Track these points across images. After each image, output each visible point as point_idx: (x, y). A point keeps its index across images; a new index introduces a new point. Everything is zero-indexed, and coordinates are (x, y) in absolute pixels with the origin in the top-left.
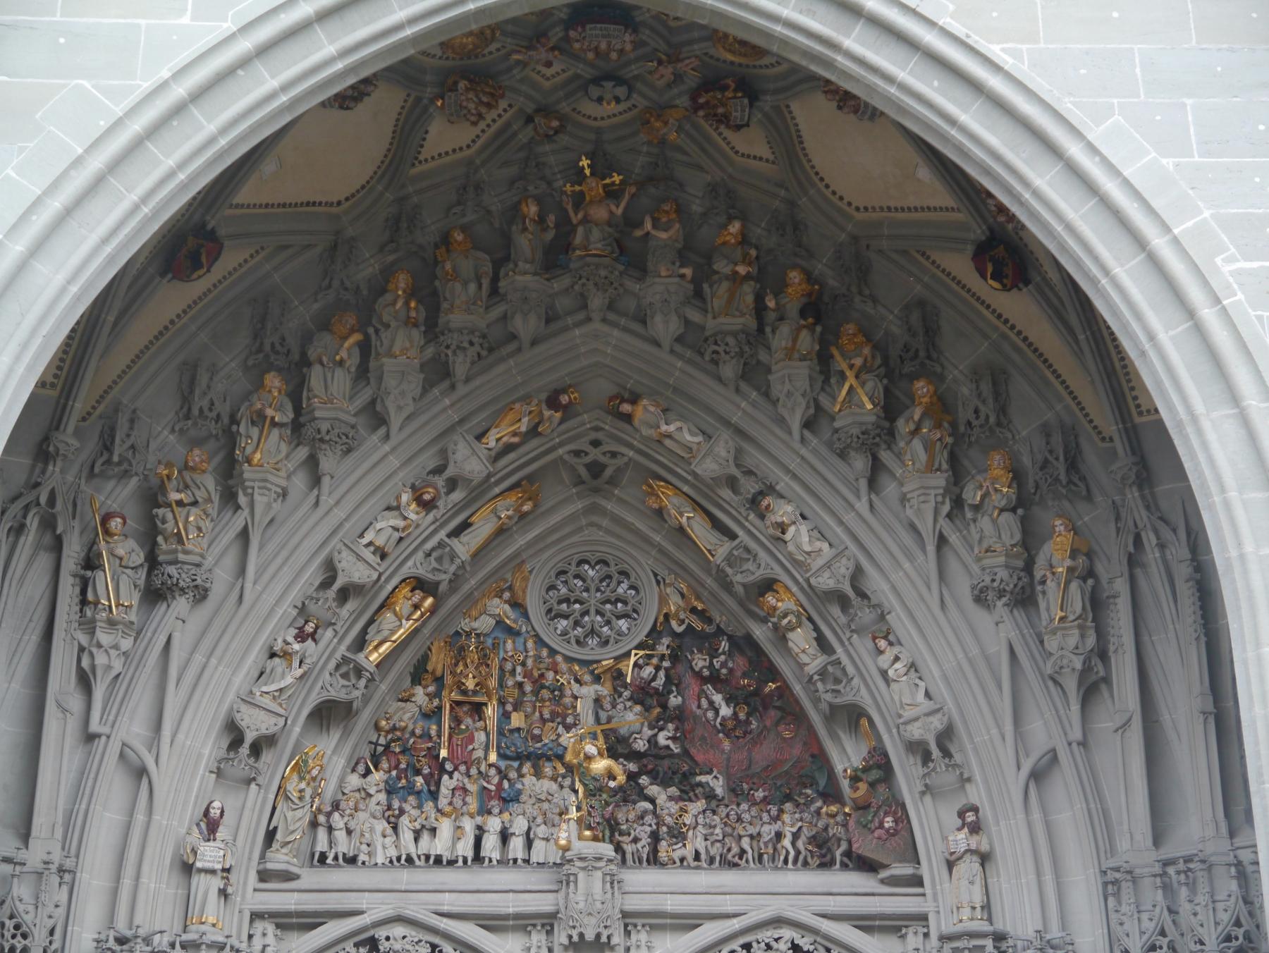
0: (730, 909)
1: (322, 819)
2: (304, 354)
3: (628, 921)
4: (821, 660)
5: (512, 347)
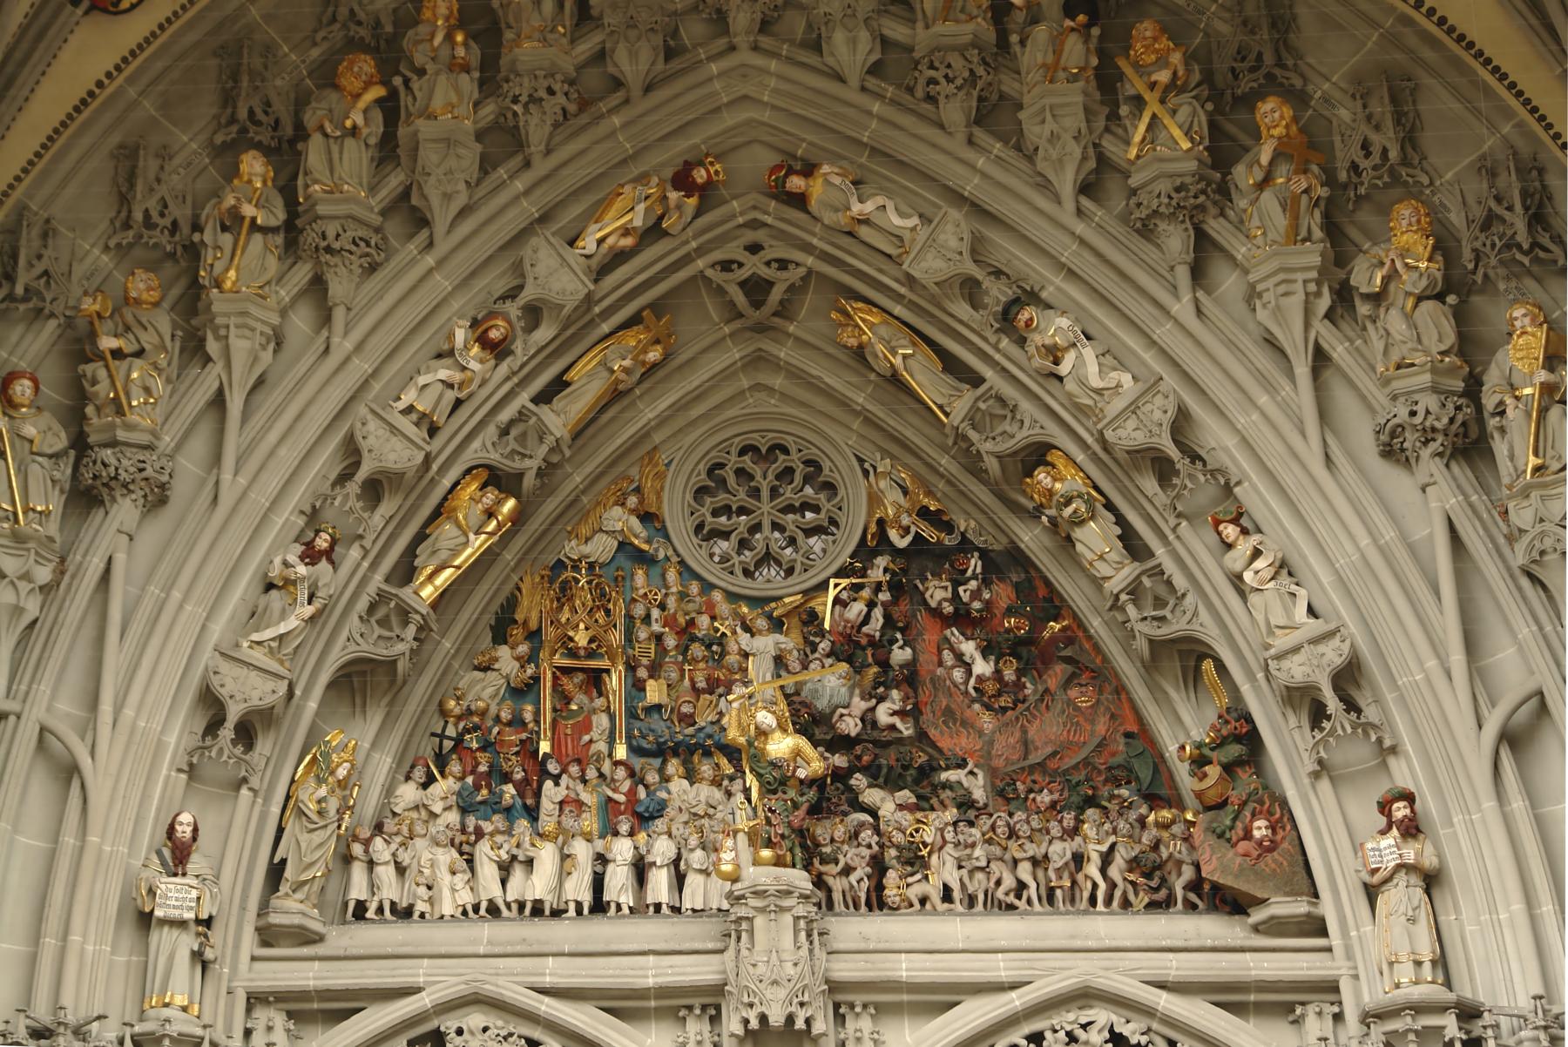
4: (1129, 570)
5: (619, 96)
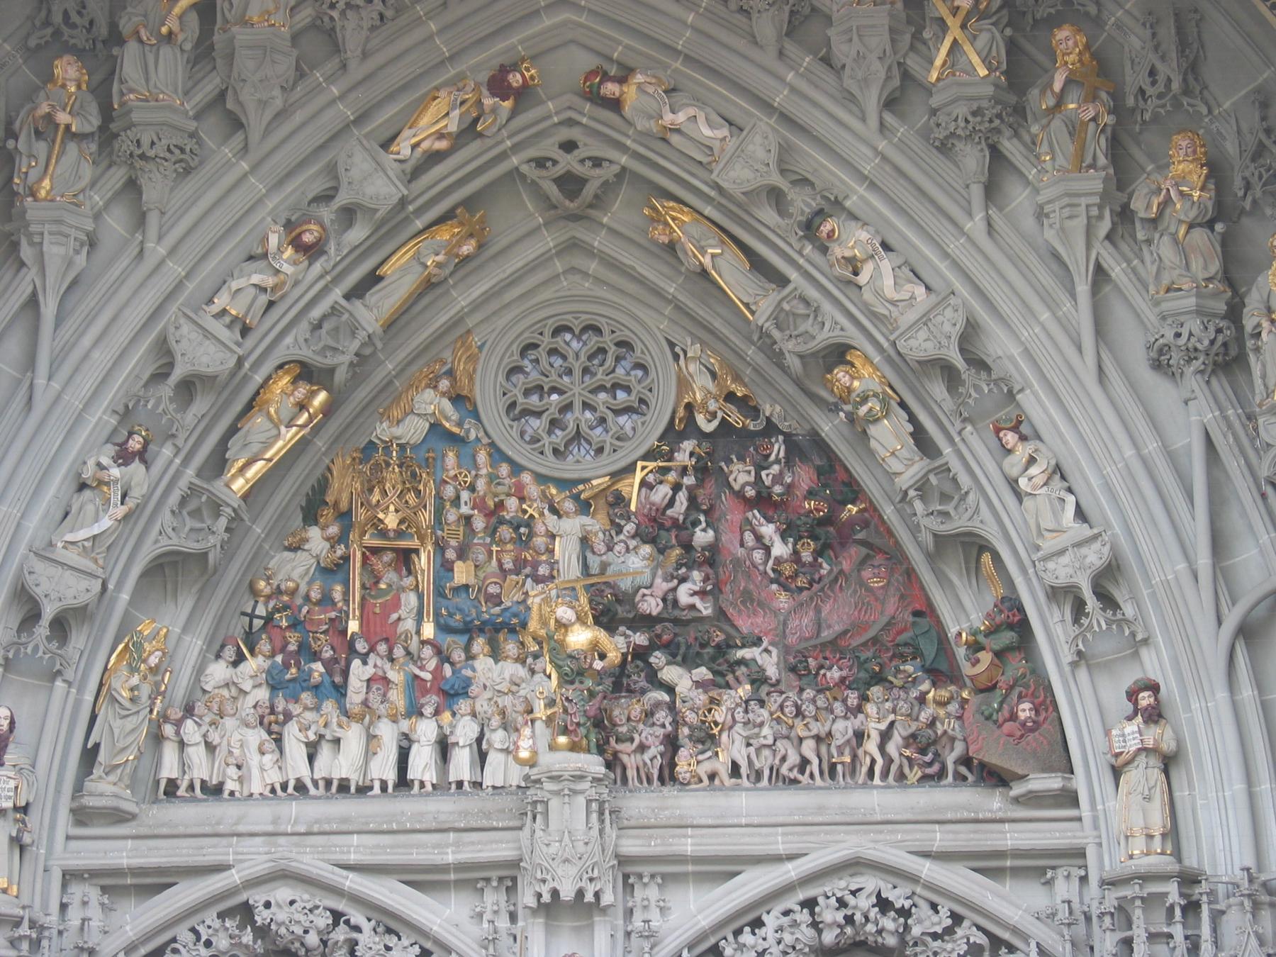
0: (781, 849)
1: (168, 730)
2: (113, 27)
3: (629, 869)
